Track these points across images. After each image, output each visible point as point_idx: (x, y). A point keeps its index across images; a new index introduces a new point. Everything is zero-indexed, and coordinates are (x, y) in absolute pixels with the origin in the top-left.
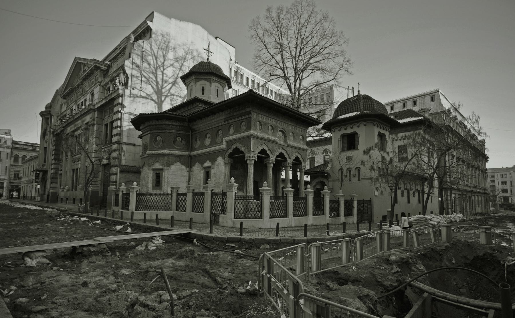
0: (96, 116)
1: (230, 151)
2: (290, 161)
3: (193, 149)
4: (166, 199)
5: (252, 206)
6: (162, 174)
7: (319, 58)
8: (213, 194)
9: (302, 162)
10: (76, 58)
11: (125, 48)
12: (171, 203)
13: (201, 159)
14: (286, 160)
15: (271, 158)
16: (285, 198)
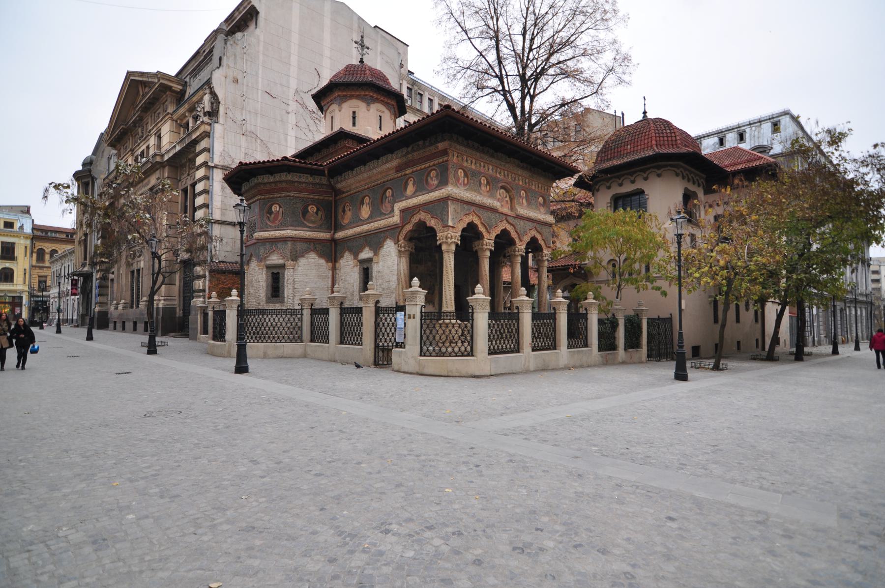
0: (166, 175)
1: (409, 227)
2: (521, 246)
3: (337, 227)
4: (292, 320)
5: (453, 331)
6: (284, 275)
7: (568, 52)
8: (378, 310)
9: (544, 247)
10: (129, 74)
11: (211, 51)
12: (301, 328)
13: (354, 245)
14: (512, 242)
15: (486, 241)
16: (515, 316)
